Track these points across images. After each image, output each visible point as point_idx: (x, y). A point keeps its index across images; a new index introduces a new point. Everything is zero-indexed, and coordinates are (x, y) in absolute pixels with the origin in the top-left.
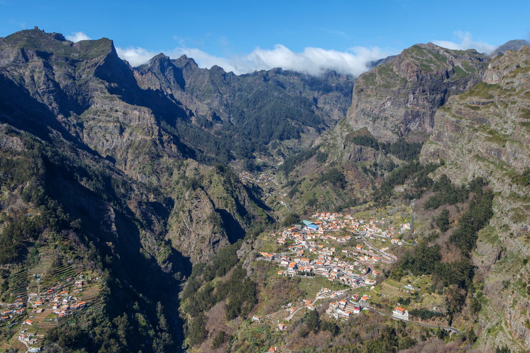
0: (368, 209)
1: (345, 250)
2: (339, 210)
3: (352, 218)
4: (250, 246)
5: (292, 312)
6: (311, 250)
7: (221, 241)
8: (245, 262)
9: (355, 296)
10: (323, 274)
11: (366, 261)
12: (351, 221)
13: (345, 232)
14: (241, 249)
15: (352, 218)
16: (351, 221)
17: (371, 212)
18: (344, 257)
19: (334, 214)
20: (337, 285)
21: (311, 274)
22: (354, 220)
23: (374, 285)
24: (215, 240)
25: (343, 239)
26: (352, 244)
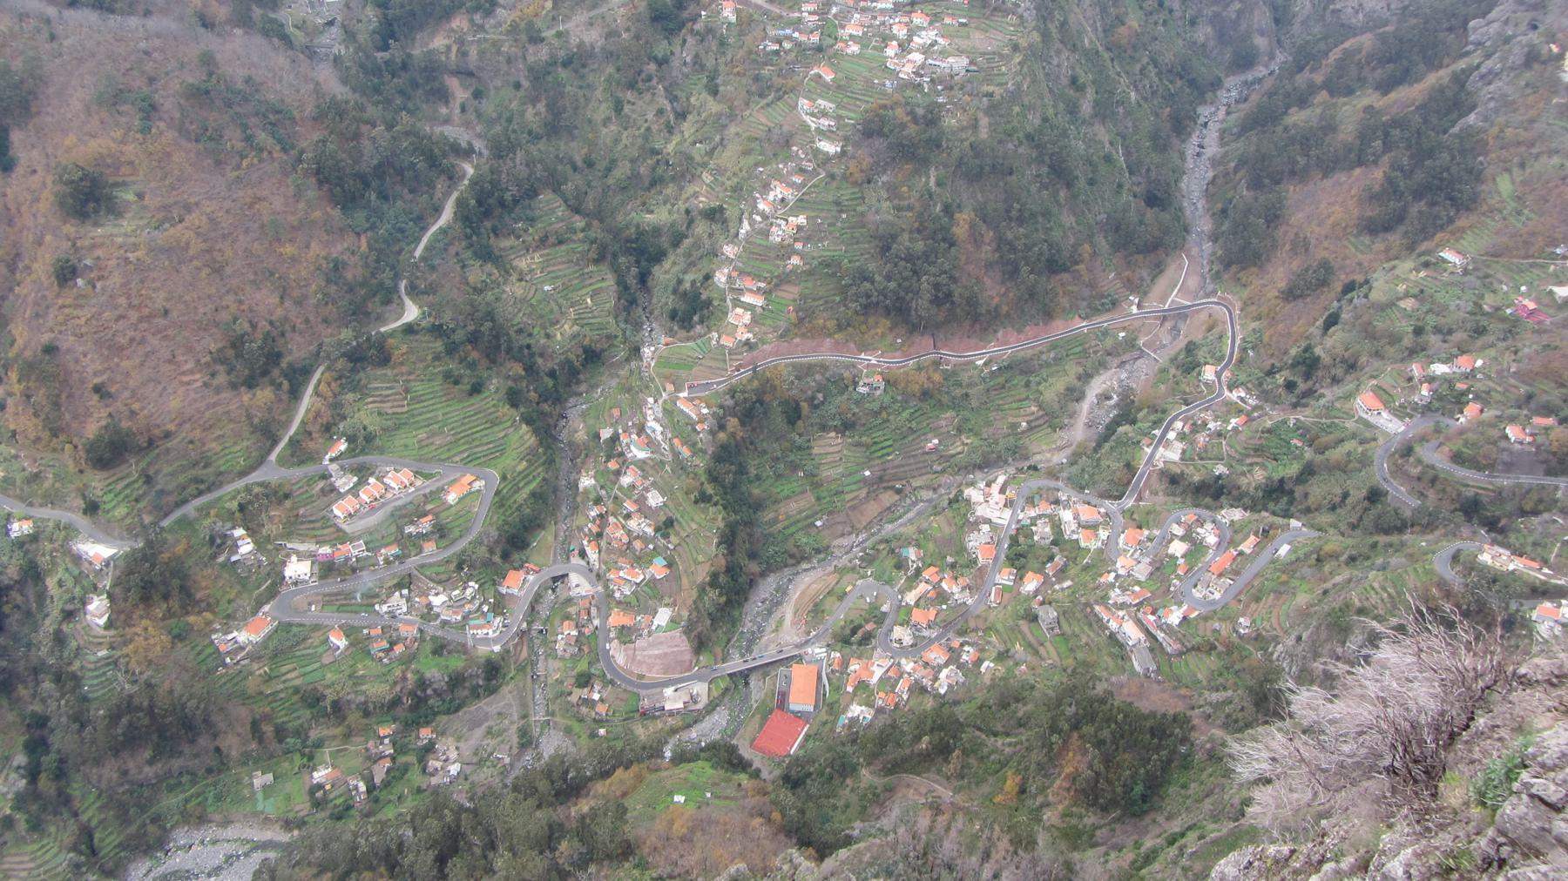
4: (1525, 17)
8: (1483, 70)
14: (1493, 15)
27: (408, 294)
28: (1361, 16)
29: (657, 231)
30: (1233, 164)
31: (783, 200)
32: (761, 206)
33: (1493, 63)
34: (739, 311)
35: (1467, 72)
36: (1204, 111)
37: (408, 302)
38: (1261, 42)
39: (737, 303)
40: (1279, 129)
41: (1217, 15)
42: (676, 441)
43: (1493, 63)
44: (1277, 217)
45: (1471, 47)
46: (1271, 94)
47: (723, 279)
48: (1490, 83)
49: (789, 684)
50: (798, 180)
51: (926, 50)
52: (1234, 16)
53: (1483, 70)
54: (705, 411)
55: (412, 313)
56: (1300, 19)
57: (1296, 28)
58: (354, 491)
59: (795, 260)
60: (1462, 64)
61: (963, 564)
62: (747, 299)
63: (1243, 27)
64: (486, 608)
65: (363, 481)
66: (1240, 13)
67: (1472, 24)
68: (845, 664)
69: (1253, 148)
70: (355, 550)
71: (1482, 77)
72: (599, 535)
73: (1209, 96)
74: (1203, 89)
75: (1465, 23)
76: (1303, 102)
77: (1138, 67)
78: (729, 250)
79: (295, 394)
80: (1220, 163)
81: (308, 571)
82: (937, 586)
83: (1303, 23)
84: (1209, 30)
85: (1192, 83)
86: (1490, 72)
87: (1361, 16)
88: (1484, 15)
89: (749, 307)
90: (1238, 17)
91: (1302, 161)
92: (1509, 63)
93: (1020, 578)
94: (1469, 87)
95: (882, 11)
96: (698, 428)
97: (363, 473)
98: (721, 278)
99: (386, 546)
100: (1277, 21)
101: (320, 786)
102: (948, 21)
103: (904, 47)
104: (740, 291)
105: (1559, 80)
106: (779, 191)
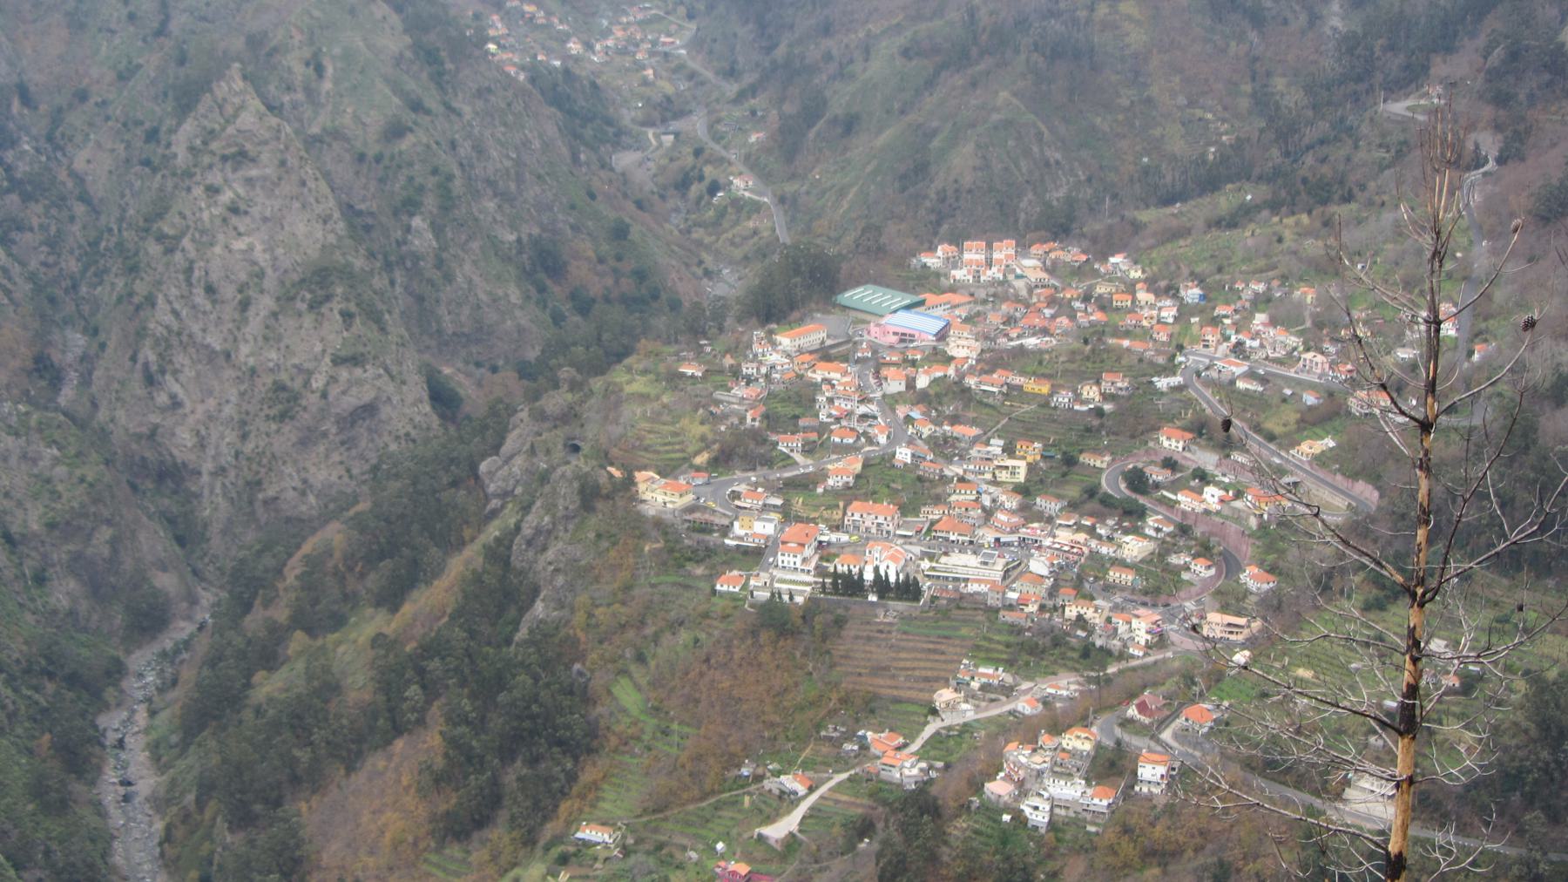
0: (1231, 223)
1: (1097, 451)
2: (1059, 227)
3: (1136, 274)
5: (799, 799)
6: (903, 455)
7: (385, 411)
8: (527, 531)
9: (1142, 708)
10: (973, 588)
11: (1207, 512)
12: (1131, 287)
13: (1091, 354)
14: (507, 448)
15: (1136, 274)
16: (1131, 287)
17: (1248, 237)
18: (1092, 492)
19: (1037, 249)
20: (1038, 648)
21: (908, 589)
22: (1151, 284)
23: (1250, 643)
24: (351, 401)
25: (1091, 392)
26: (1133, 420)
28: (312, 499)
30: (190, 798)
36: (111, 722)
38: (166, 582)
40: (248, 715)
41: (77, 557)
44: (297, 862)
46: (213, 661)
48: (544, 549)
52: (106, 551)
53: (527, 531)
56: (215, 528)
57: (216, 543)
60: (493, 531)
63: (128, 565)
66: (114, 543)
67: (483, 467)
69: (215, 760)
71: (529, 543)
73: (110, 694)
74: (95, 685)
75: (474, 468)
76: (269, 658)
80: (169, 802)
83: (224, 532)
84: (72, 584)
85: (73, 680)
86: (538, 531)
87: (312, 499)
88: (496, 449)
90: (115, 551)
91: (303, 755)
92: (561, 512)
94: (516, 562)
100: (181, 541)
105: (640, 517)
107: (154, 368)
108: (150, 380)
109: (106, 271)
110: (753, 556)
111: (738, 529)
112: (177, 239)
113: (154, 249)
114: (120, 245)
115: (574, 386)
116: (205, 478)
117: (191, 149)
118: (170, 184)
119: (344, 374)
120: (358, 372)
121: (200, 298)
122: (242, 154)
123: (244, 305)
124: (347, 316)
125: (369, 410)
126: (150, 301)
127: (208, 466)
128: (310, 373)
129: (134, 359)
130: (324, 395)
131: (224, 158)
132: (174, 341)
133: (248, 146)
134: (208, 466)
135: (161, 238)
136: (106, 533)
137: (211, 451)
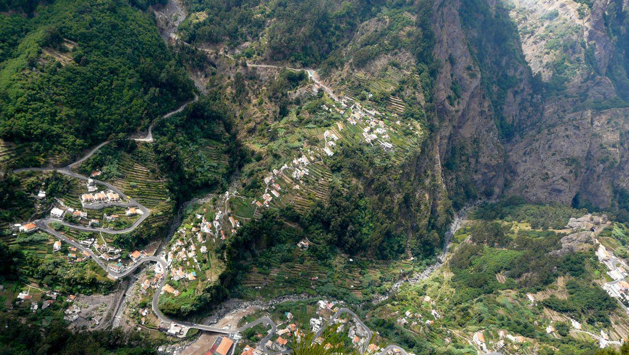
4: (591, 225)
7: (563, 194)
8: (569, 237)
14: (579, 219)
24: (558, 187)
27: (152, 132)
28: (535, 197)
29: (253, 152)
31: (303, 163)
32: (294, 161)
33: (574, 236)
34: (268, 195)
35: (565, 235)
37: (150, 134)
38: (497, 190)
39: (269, 192)
41: (486, 173)
42: (222, 231)
43: (574, 236)
45: (567, 226)
47: (268, 181)
48: (570, 242)
49: (219, 344)
50: (312, 158)
51: (378, 135)
52: (491, 176)
53: (569, 237)
54: (238, 226)
55: (149, 139)
56: (512, 188)
57: (511, 191)
58: (94, 193)
59: (297, 187)
60: (562, 231)
61: (305, 327)
62: (273, 192)
63: (493, 182)
64: (120, 260)
65: (99, 191)
66: (494, 176)
67: (571, 219)
68: (243, 346)
70: (83, 214)
71: (568, 239)
72: (176, 253)
73: (471, 200)
77: (451, 177)
78: (275, 171)
79: (90, 147)
81: (60, 214)
82: (292, 332)
83: (514, 190)
85: (467, 193)
86: (571, 238)
87: (535, 197)
88: (577, 218)
89: (272, 195)
90: (493, 177)
92: (579, 239)
93: (325, 343)
94: (562, 240)
95: (370, 115)
96: (233, 231)
97: (101, 188)
98: (267, 180)
99: (95, 219)
100: (505, 185)
101: (20, 300)
102: (391, 129)
103: (371, 131)
104: (273, 188)
106: (304, 159)
107: (527, 152)
108: (525, 154)
109: (534, 129)
110: (611, 280)
111: (612, 272)
112: (552, 133)
113: (546, 131)
114: (541, 126)
115: (604, 219)
116: (519, 178)
117: (569, 119)
118: (559, 122)
119: (561, 181)
120: (565, 183)
121: (547, 146)
122: (578, 127)
123: (554, 154)
124: (571, 171)
125: (560, 191)
126: (537, 140)
127: (521, 177)
128: (555, 176)
129: (525, 148)
130: (554, 182)
131: (574, 125)
132: (535, 151)
133: (581, 127)
134: (521, 177)
135: (549, 131)
136: (494, 173)
137: (524, 174)
